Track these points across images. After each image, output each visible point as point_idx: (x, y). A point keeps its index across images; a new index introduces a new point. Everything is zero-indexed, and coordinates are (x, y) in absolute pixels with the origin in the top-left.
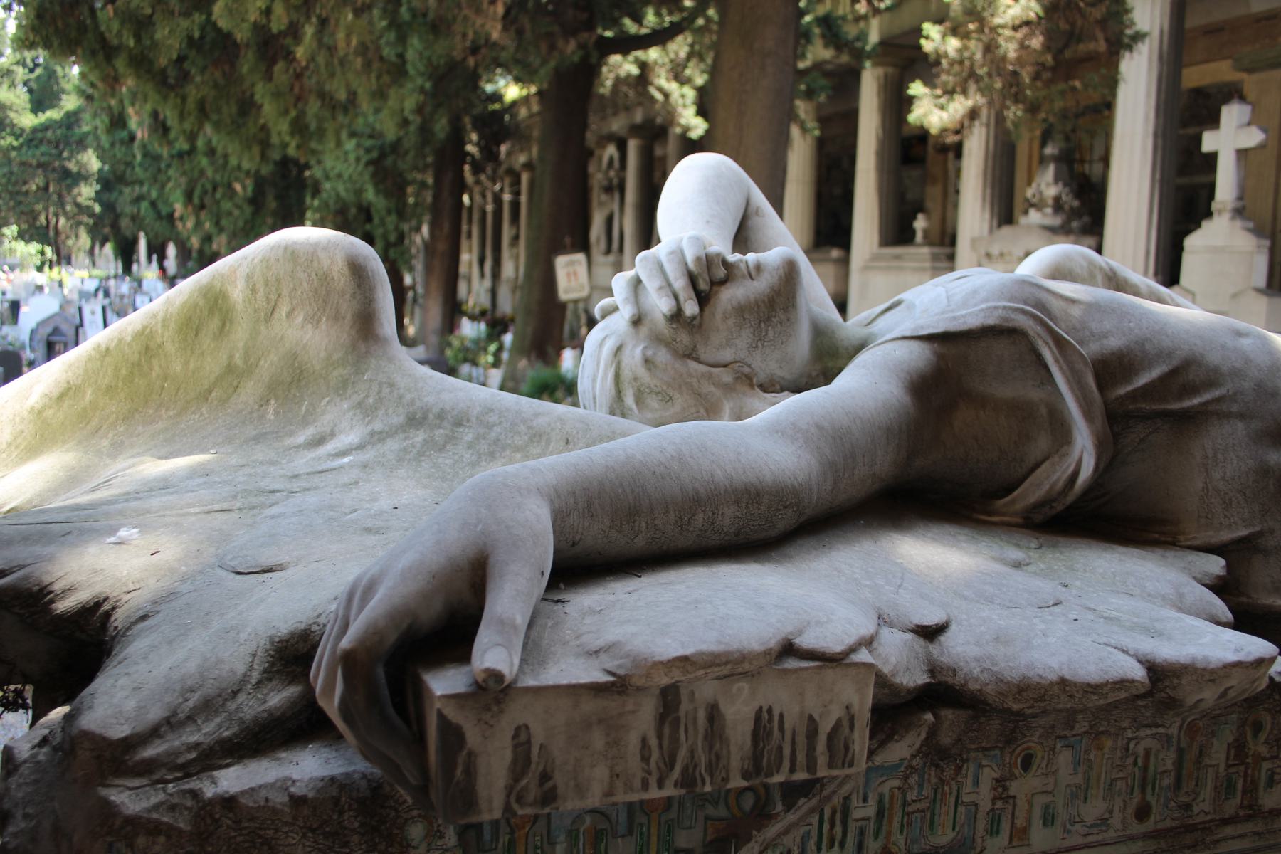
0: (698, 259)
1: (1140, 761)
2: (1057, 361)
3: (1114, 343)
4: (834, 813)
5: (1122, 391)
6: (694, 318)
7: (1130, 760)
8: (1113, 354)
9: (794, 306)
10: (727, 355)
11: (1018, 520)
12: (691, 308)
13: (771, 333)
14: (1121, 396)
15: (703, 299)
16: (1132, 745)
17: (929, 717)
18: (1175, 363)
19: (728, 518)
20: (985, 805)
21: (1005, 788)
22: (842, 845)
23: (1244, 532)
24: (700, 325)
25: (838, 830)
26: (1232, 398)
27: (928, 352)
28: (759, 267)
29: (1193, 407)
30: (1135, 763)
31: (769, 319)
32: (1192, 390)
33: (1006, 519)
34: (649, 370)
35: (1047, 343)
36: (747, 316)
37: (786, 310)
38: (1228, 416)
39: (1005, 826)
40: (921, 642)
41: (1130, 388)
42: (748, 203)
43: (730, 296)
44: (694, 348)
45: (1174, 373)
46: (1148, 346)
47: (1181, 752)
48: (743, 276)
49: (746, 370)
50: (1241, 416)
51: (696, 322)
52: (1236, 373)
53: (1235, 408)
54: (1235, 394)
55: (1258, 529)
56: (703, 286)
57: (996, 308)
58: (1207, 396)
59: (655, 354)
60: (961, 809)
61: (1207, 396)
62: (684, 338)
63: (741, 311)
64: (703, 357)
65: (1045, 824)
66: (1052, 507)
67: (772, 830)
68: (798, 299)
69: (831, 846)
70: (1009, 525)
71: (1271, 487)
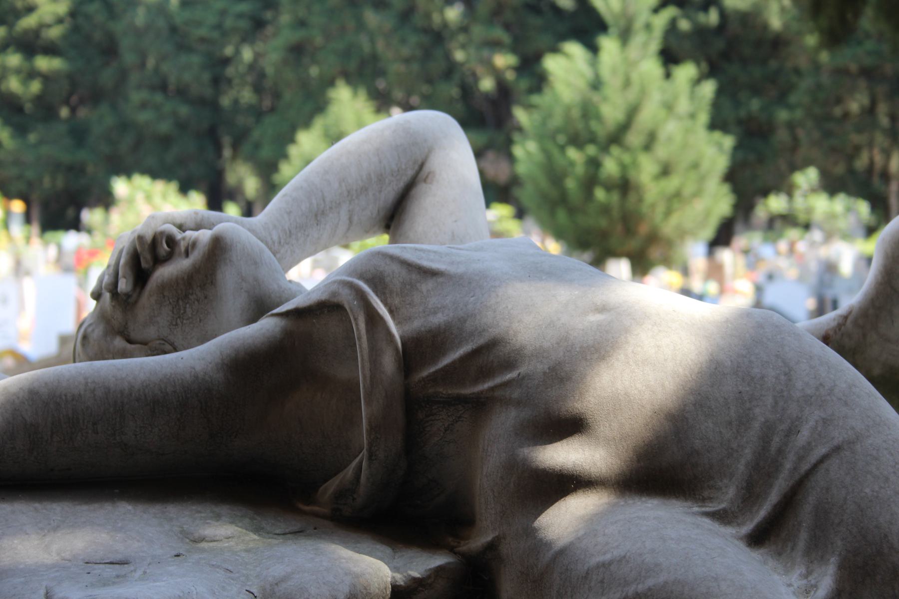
0: (140, 238)
2: (360, 338)
3: (438, 319)
5: (425, 373)
6: (128, 295)
8: (430, 331)
9: (213, 283)
10: (151, 332)
11: (326, 511)
12: (124, 285)
13: (189, 310)
14: (423, 379)
18: (481, 341)
23: (488, 538)
24: (136, 302)
26: (519, 381)
27: (278, 329)
28: (194, 244)
29: (482, 392)
31: (186, 296)
32: (486, 373)
33: (316, 508)
34: (83, 345)
35: (355, 319)
36: (166, 293)
37: (203, 287)
38: (507, 402)
41: (433, 369)
42: (422, 166)
44: (126, 327)
45: (476, 353)
46: (469, 326)
48: (180, 254)
50: (518, 403)
51: (131, 300)
52: (540, 354)
53: (516, 394)
54: (523, 378)
55: (497, 534)
56: (144, 265)
57: (335, 282)
58: (498, 380)
59: (93, 330)
61: (498, 380)
62: (119, 315)
63: (163, 287)
64: (133, 336)
66: (354, 499)
68: (219, 276)
71: (512, 485)
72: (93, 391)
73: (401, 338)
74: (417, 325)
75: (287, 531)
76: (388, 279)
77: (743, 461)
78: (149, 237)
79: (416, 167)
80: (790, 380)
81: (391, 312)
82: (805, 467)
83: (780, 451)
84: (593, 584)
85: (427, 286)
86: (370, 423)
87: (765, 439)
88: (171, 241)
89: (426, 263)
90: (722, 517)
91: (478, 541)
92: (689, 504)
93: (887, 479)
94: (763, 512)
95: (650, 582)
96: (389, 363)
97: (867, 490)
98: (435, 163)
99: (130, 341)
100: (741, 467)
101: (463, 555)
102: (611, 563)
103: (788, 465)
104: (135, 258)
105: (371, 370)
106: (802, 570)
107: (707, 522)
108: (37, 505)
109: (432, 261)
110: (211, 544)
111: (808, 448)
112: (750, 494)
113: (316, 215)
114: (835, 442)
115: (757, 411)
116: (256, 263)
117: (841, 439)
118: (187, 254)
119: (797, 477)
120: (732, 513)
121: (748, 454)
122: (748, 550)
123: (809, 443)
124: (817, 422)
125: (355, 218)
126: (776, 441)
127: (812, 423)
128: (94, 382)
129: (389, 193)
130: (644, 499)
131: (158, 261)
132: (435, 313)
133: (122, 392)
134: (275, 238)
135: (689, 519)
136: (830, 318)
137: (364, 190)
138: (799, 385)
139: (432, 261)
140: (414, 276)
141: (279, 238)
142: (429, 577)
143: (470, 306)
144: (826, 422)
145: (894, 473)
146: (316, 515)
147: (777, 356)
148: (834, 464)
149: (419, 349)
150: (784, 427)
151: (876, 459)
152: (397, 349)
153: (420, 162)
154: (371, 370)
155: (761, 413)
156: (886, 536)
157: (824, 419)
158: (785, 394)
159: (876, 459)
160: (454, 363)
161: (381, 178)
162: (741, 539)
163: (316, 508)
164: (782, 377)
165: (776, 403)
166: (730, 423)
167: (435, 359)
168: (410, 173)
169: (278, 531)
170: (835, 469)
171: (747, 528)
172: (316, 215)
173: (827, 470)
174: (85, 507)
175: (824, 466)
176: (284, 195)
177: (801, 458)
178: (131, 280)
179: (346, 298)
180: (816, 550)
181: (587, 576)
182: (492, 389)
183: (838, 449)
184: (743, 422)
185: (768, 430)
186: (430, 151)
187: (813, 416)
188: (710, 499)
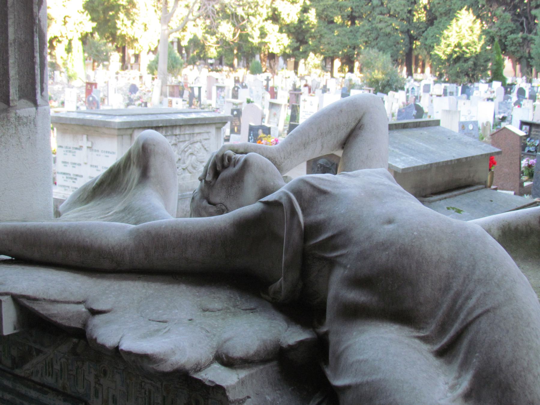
1: (147, 393)
3: (321, 217)
4: (49, 363)
6: (210, 182)
7: (143, 391)
8: (315, 223)
9: (243, 181)
12: (209, 178)
15: (216, 174)
16: (143, 384)
17: (75, 340)
18: (335, 232)
19: (74, 257)
20: (93, 385)
21: (99, 380)
22: (52, 376)
24: (213, 186)
25: (51, 369)
28: (238, 161)
30: (145, 394)
31: (231, 186)
32: (335, 248)
37: (238, 182)
39: (100, 396)
40: (89, 314)
42: (359, 121)
43: (225, 174)
45: (332, 237)
47: (164, 399)
49: (224, 207)
51: (212, 184)
56: (218, 169)
60: (85, 381)
63: (223, 180)
65: (113, 402)
67: (34, 361)
68: (245, 178)
69: (49, 375)
70: (269, 301)
72: (174, 234)
73: (305, 223)
74: (312, 218)
75: (248, 308)
76: (303, 194)
77: (442, 311)
78: (220, 155)
79: (357, 122)
80: (474, 269)
81: (303, 210)
82: (470, 318)
83: (461, 308)
84: (353, 370)
85: (320, 198)
86: (285, 263)
87: (454, 301)
88: (230, 158)
89: (322, 187)
90: (425, 339)
91: (324, 329)
92: (412, 330)
93: (508, 331)
94: (445, 340)
95: (374, 377)
96: (296, 236)
97: (496, 337)
98: (365, 121)
99: (210, 203)
100: (440, 314)
101: (318, 334)
102: (362, 361)
103: (462, 316)
104: (214, 165)
105: (290, 238)
106: (455, 374)
107: (417, 341)
108: (146, 284)
109: (324, 185)
110: (210, 313)
111: (473, 309)
112: (443, 329)
113: (304, 145)
114: (487, 307)
115: (454, 284)
116: (264, 172)
117: (490, 306)
118: (234, 166)
119: (465, 324)
120: (432, 337)
121: (445, 307)
122: (434, 359)
123: (474, 306)
124: (481, 294)
125: (325, 145)
126: (460, 302)
127: (478, 295)
128: (175, 229)
129: (343, 134)
130: (392, 324)
131: (224, 167)
132: (320, 213)
133: (187, 235)
134: (282, 156)
135: (407, 341)
136: (273, 384)
137: (330, 132)
138: (477, 272)
139: (324, 185)
140: (316, 193)
141: (285, 156)
142: (295, 345)
143: (335, 212)
144: (485, 294)
145: (512, 328)
146: (266, 300)
147: (471, 255)
148: (484, 319)
149: (311, 230)
150: (464, 295)
151: (505, 319)
152: (301, 228)
153: (358, 119)
154: (290, 238)
155: (456, 286)
156: (500, 363)
157: (484, 293)
158: (470, 277)
159: (505, 319)
160: (323, 240)
161: (338, 127)
162: (432, 352)
163: (267, 297)
164: (471, 267)
165: (464, 281)
166: (440, 289)
167: (317, 237)
168: (353, 124)
169: (244, 308)
170: (484, 323)
171: (437, 347)
172: (304, 145)
173: (480, 322)
174: (166, 287)
175: (477, 322)
176: (291, 135)
177: (469, 314)
178: (212, 175)
179: (284, 201)
180: (464, 366)
181: (352, 365)
182: (337, 257)
183: (487, 311)
184: (447, 288)
185: (458, 294)
186: (364, 114)
187: (480, 291)
188: (423, 328)
